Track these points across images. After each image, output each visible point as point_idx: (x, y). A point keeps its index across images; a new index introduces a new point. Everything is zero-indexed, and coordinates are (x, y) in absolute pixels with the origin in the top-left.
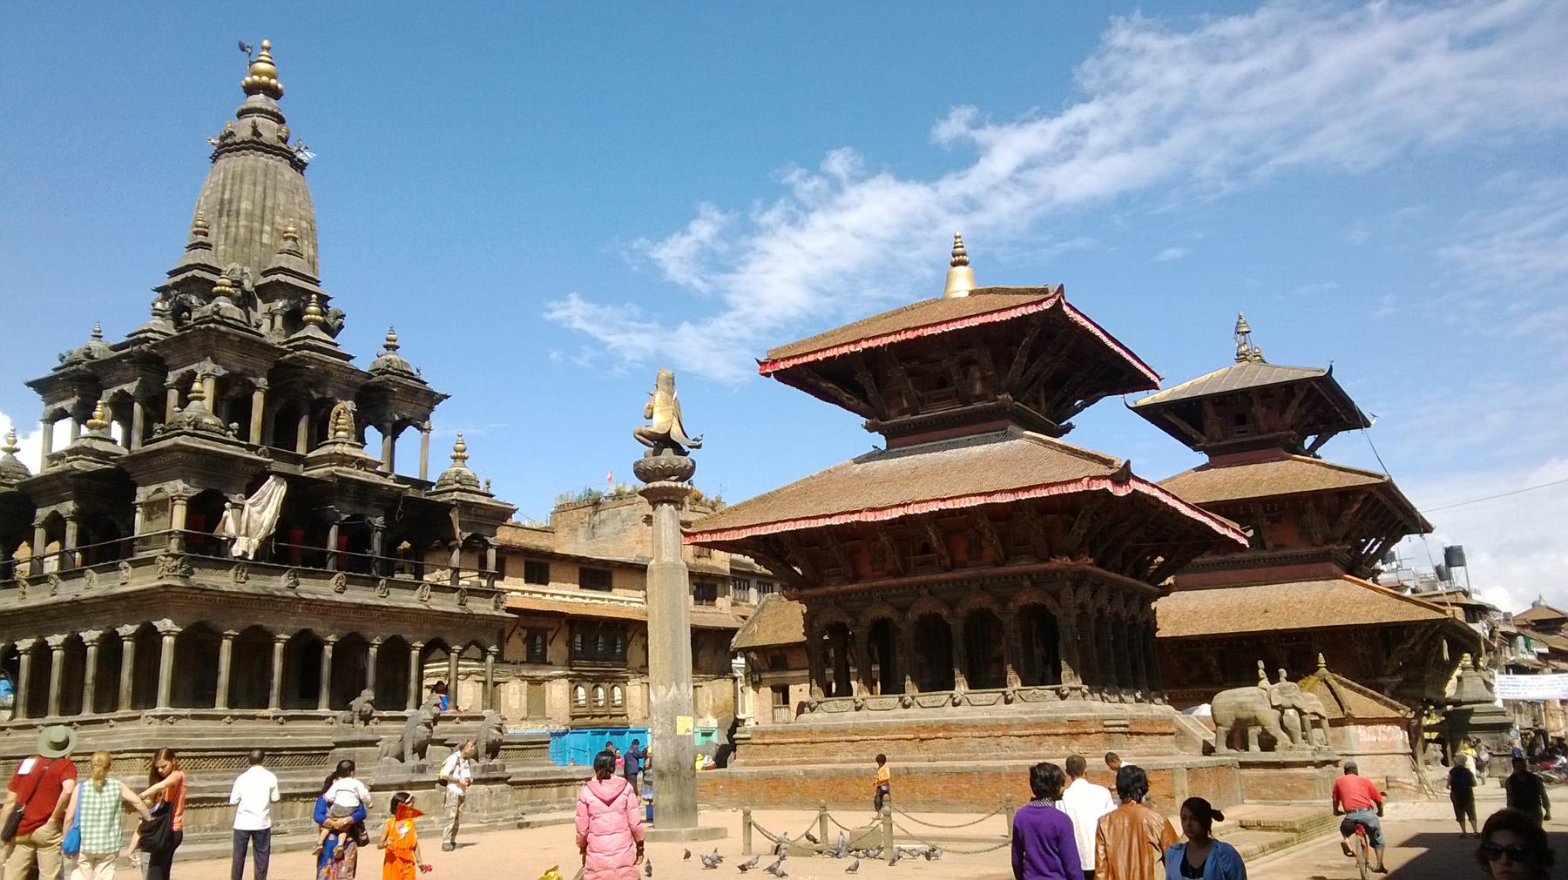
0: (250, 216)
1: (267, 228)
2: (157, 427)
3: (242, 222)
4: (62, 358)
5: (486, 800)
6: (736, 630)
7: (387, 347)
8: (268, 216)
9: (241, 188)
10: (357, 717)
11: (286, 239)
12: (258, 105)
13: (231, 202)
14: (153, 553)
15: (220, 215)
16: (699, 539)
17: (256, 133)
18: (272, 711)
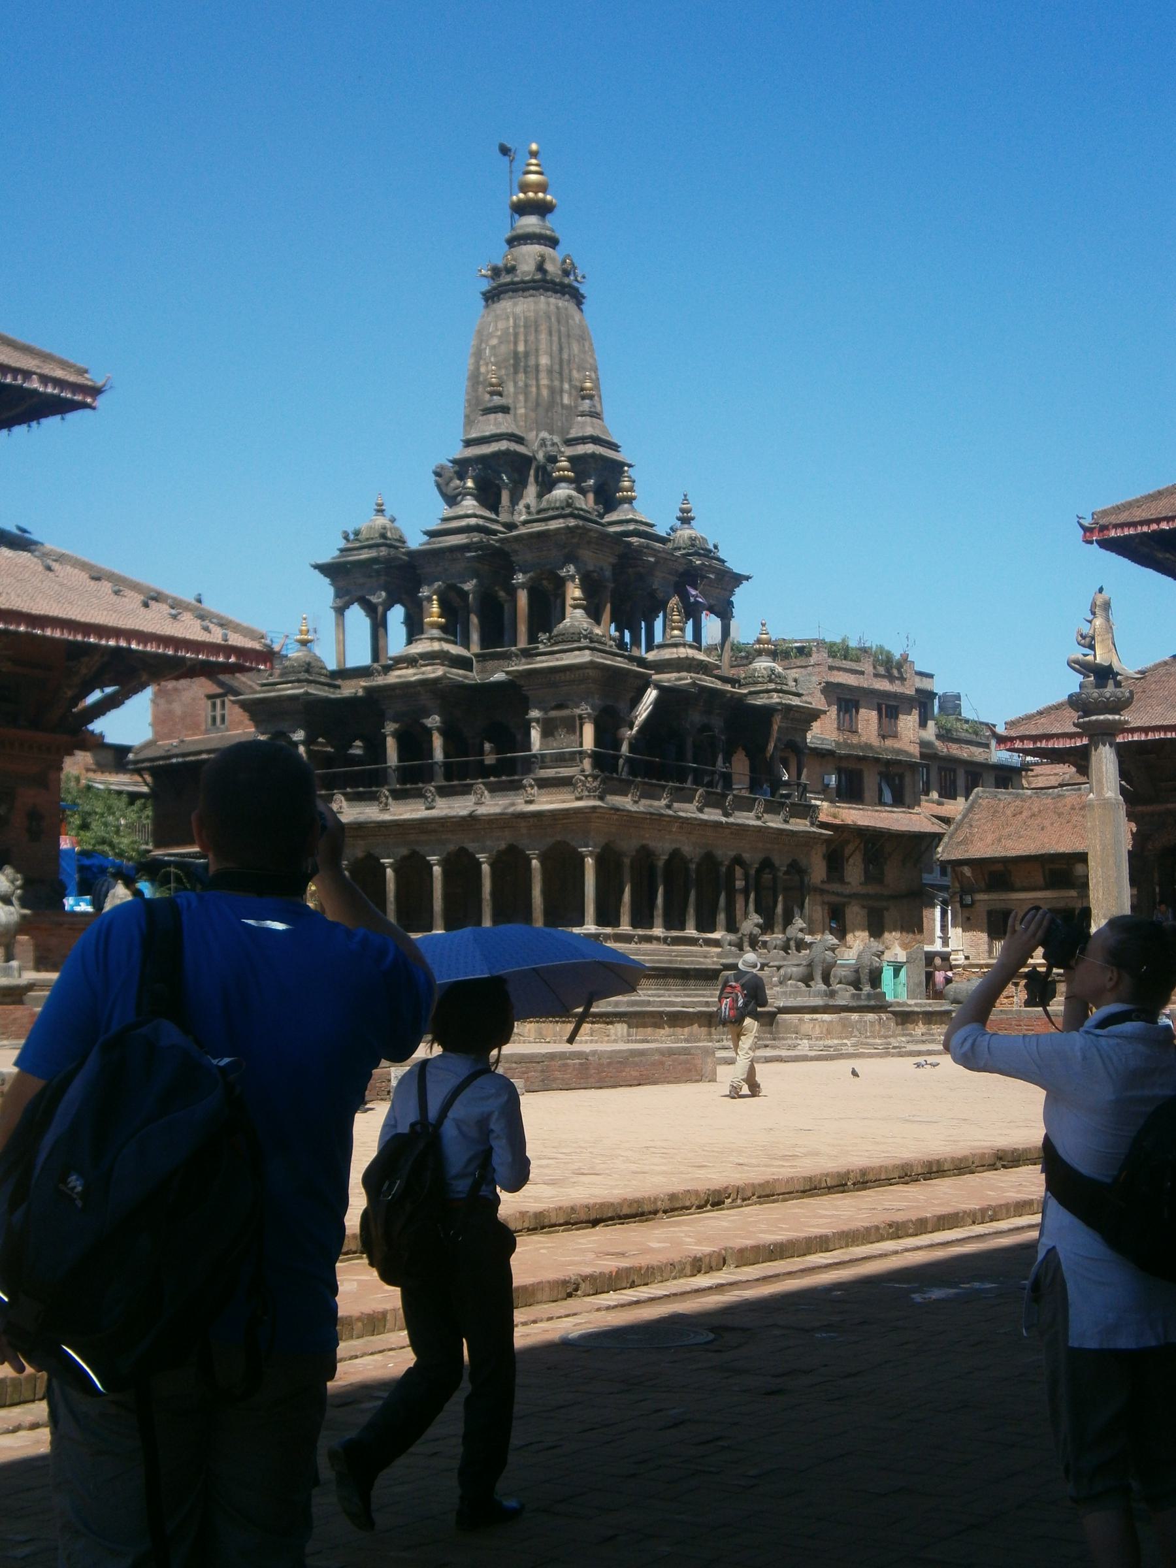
0: (550, 371)
1: (566, 386)
2: (543, 637)
3: (544, 381)
4: (346, 538)
5: (877, 1027)
6: (943, 834)
7: (679, 519)
8: (566, 371)
9: (537, 340)
10: (746, 939)
11: (583, 398)
12: (530, 230)
13: (527, 354)
14: (565, 772)
15: (516, 372)
16: (1018, 745)
17: (540, 268)
18: (658, 931)
